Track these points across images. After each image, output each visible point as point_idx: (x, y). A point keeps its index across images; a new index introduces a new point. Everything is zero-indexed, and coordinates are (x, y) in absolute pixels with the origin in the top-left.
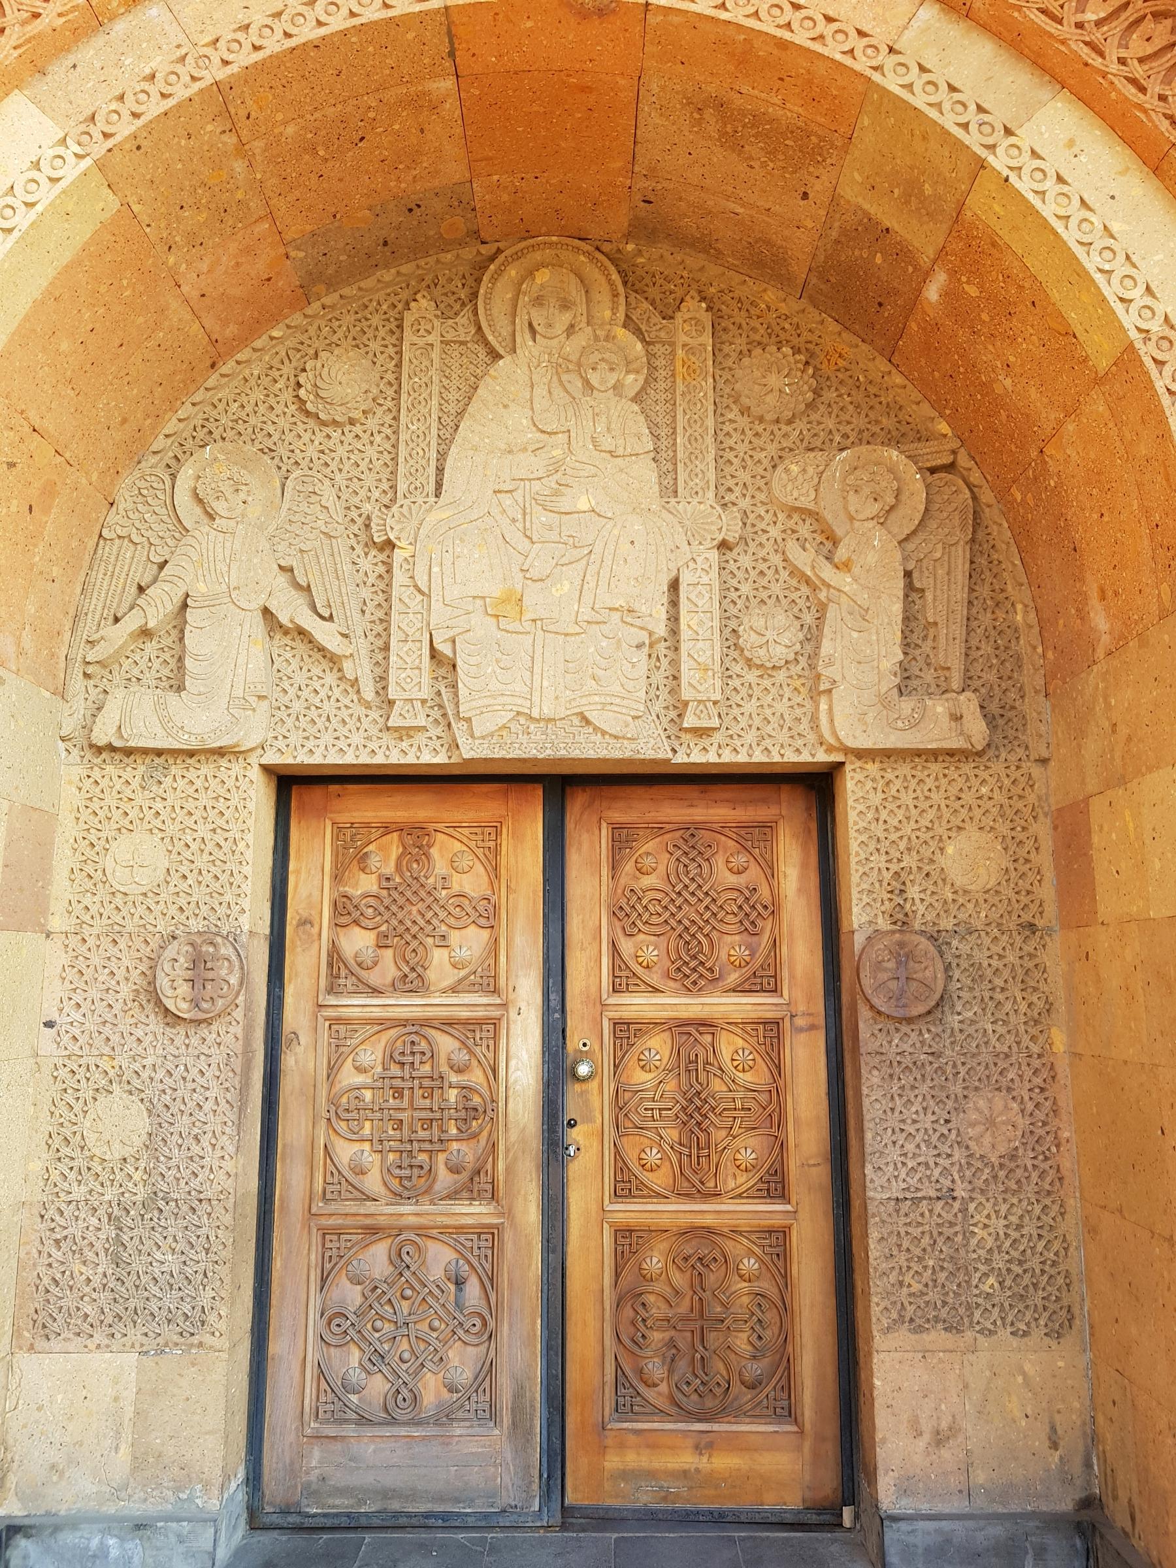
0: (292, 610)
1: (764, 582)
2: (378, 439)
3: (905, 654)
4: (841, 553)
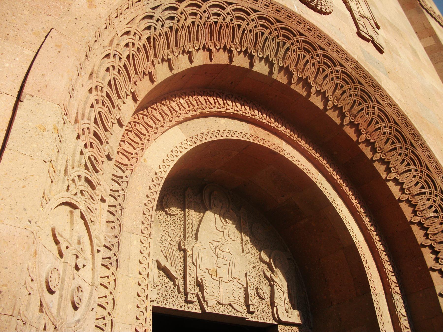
0: (164, 263)
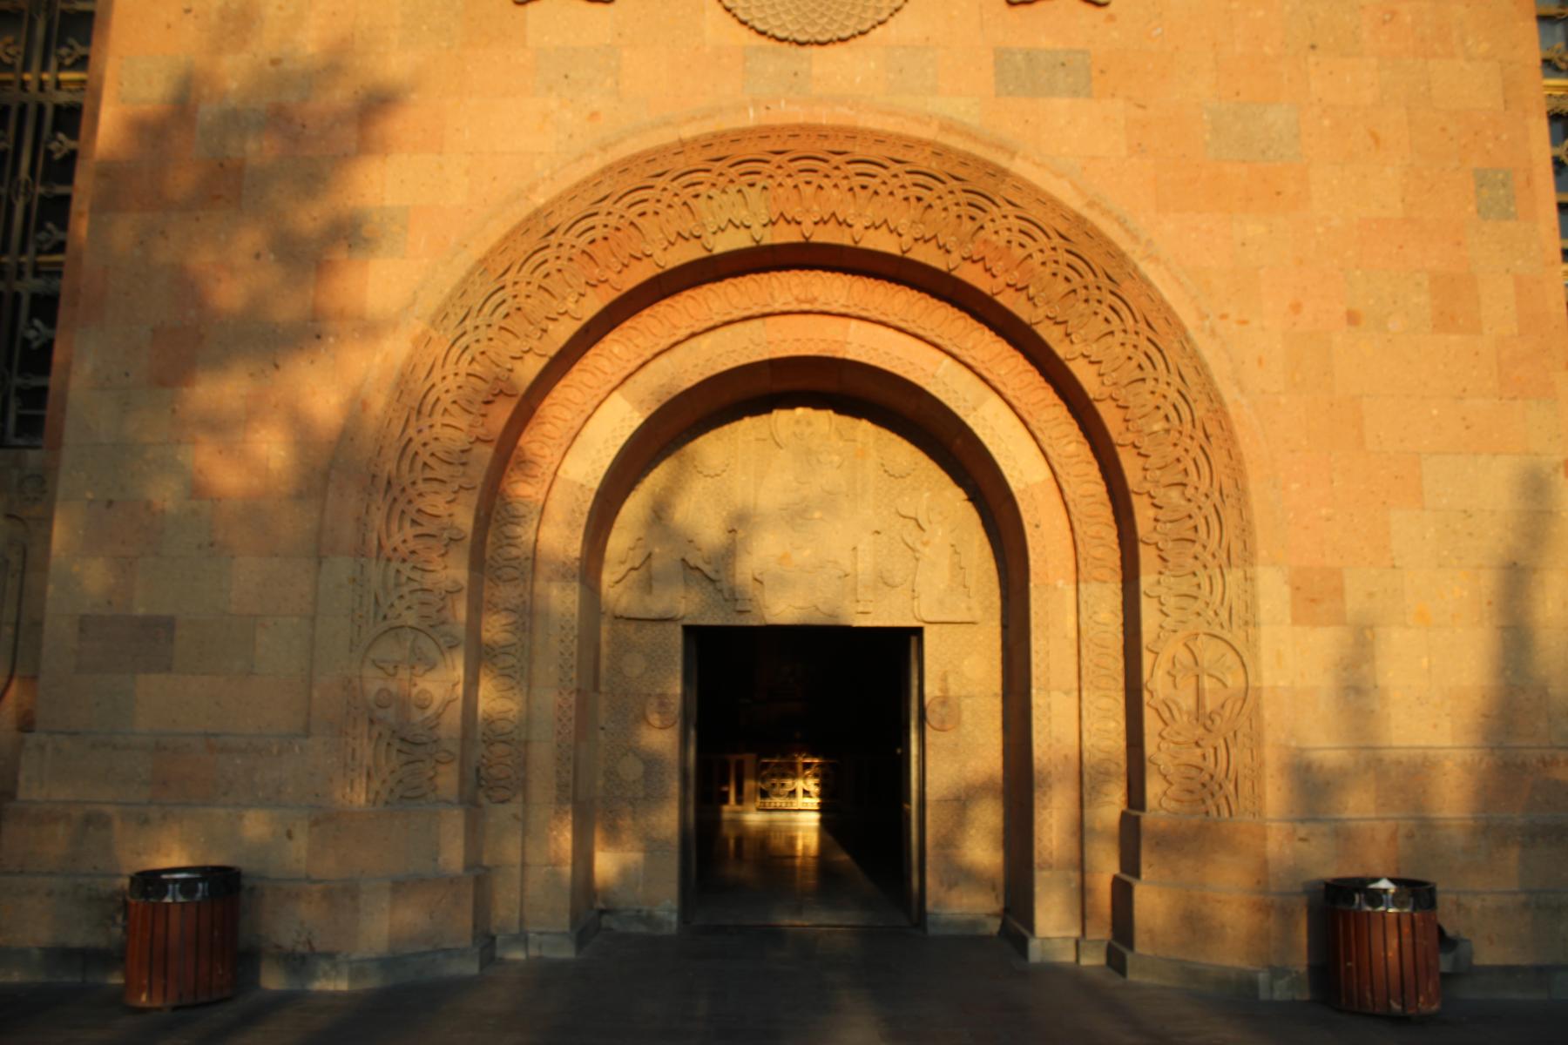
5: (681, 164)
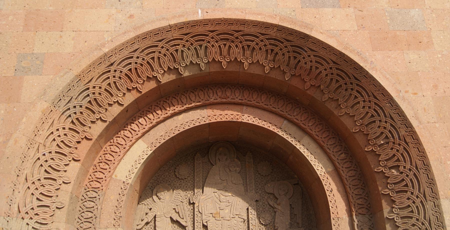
1: (264, 207)
2: (190, 182)
3: (291, 220)
4: (278, 202)
5: (170, 36)
